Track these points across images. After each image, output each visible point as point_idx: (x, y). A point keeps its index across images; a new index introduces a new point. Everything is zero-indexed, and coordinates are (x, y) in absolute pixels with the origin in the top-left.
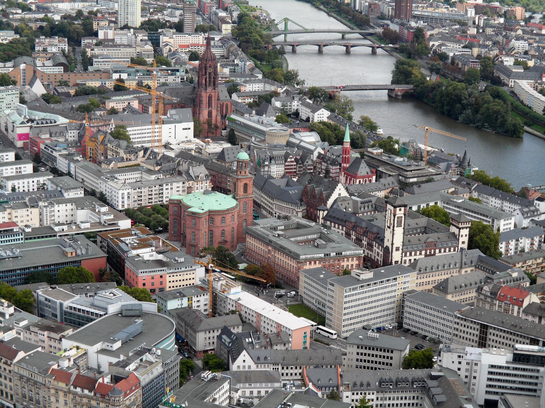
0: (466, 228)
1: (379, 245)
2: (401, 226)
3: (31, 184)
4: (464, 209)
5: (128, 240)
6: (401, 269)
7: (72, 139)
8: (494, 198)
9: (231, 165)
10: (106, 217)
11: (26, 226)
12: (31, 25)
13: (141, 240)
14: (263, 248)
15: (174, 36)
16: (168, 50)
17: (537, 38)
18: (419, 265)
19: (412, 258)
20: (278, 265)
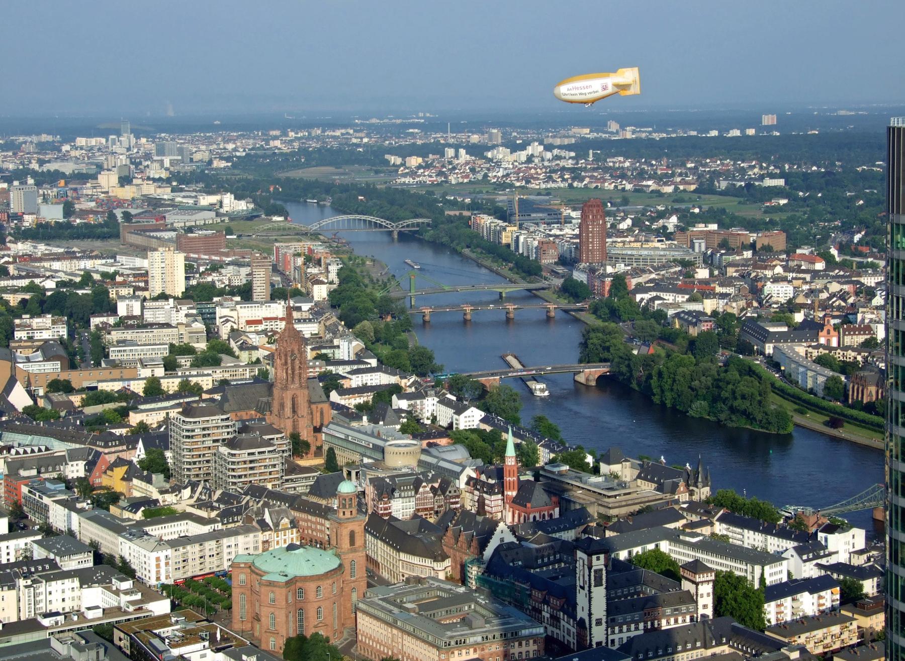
0: (708, 581)
2: (602, 585)
5: (166, 632)
7: (75, 475)
8: (751, 532)
12: (6, 296)
15: (238, 307)
16: (229, 328)
17: (808, 277)
19: (625, 636)
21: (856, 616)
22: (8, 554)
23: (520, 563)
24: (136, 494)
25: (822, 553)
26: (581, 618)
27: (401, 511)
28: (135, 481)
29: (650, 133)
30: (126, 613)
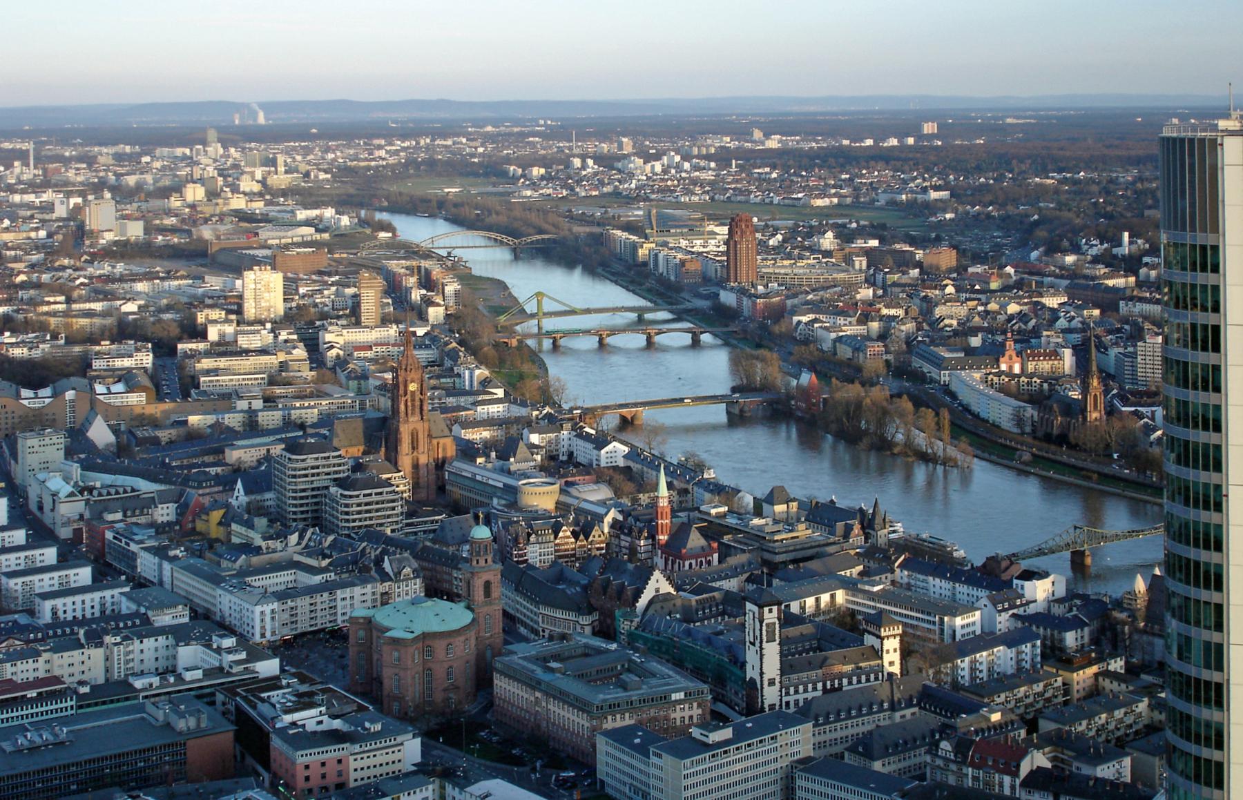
0: (894, 636)
3: (88, 605)
5: (276, 696)
6: (783, 718)
7: (165, 519)
8: (937, 580)
9: (458, 550)
10: (232, 657)
11: (81, 683)
13: (300, 695)
14: (526, 696)
19: (801, 697)
20: (554, 724)
21: (1060, 672)
22: (93, 607)
24: (235, 540)
25: (1018, 602)
28: (234, 526)
29: (798, 142)
30: (229, 674)
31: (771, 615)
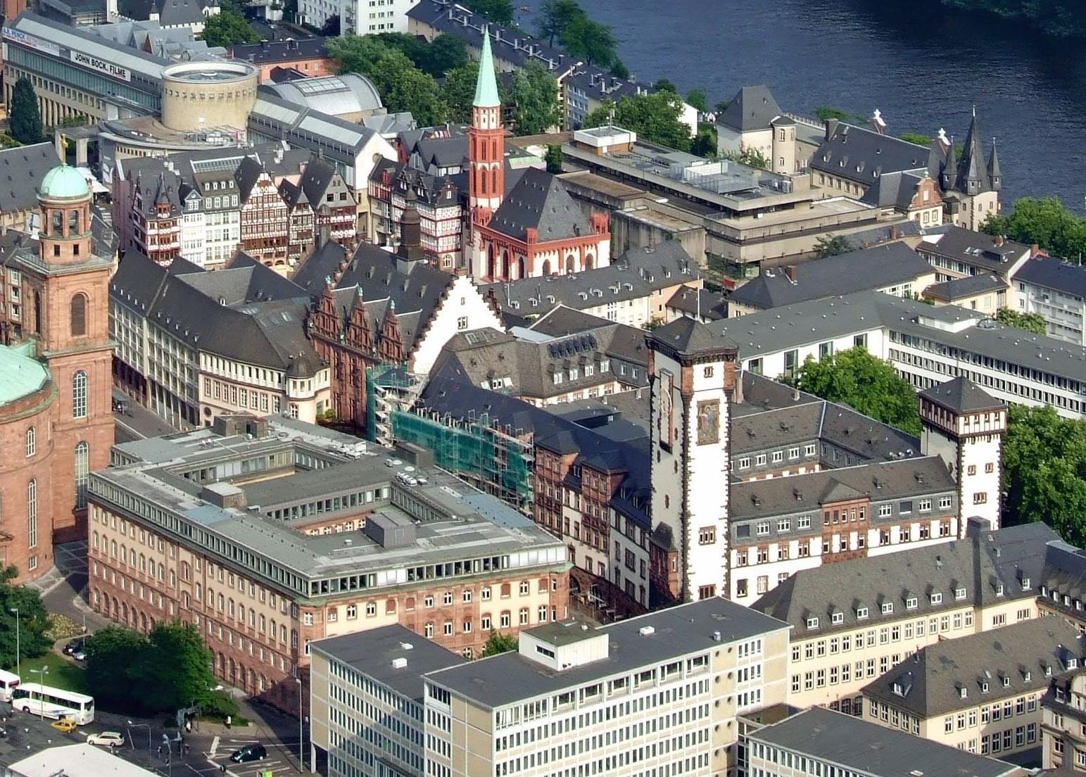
0: (989, 434)
1: (630, 521)
2: (716, 441)
4: (977, 359)
14: (159, 559)
18: (798, 600)
23: (508, 382)
26: (662, 526)
27: (205, 245)
31: (710, 383)
